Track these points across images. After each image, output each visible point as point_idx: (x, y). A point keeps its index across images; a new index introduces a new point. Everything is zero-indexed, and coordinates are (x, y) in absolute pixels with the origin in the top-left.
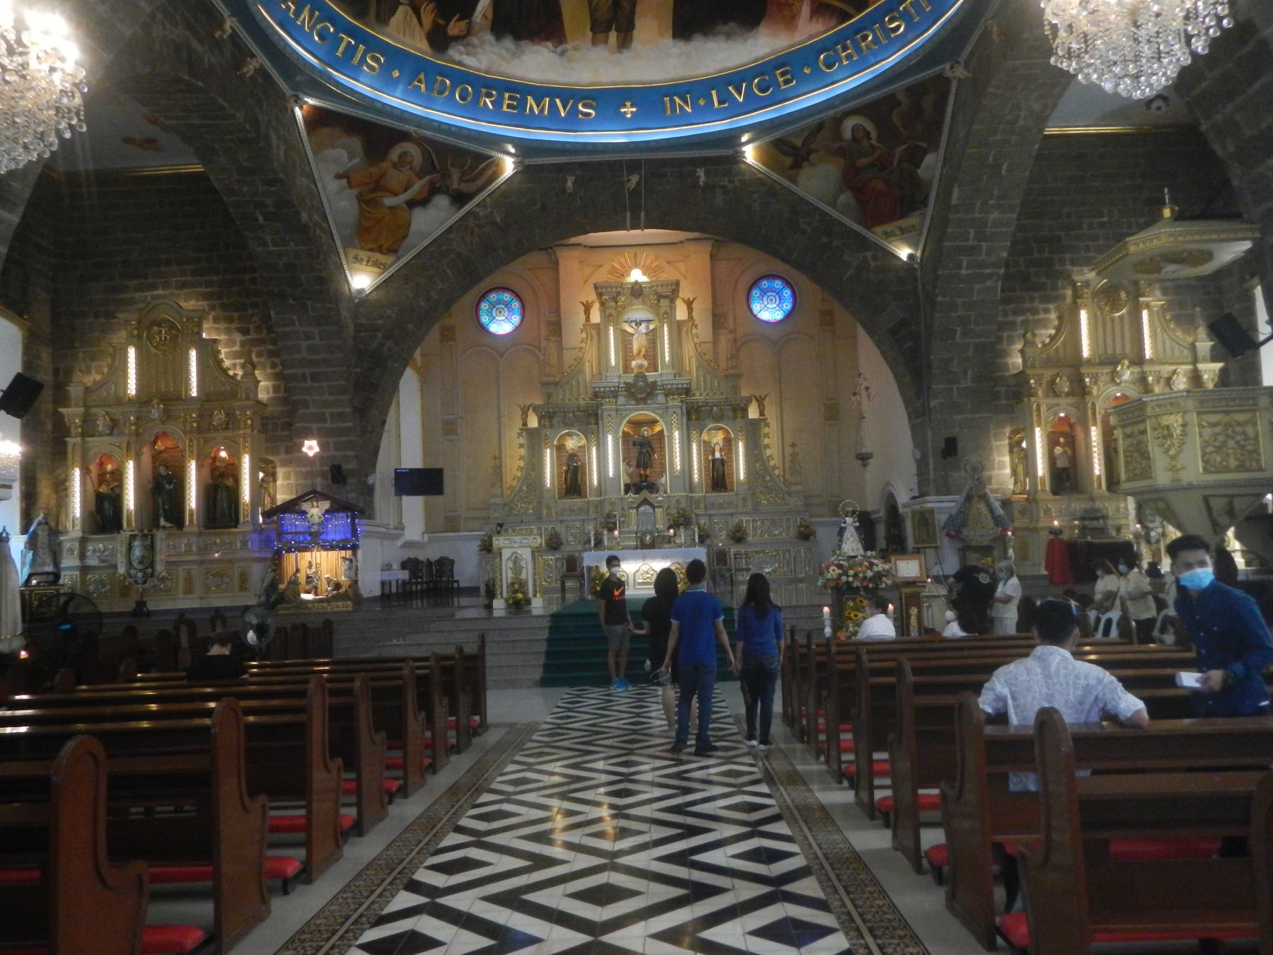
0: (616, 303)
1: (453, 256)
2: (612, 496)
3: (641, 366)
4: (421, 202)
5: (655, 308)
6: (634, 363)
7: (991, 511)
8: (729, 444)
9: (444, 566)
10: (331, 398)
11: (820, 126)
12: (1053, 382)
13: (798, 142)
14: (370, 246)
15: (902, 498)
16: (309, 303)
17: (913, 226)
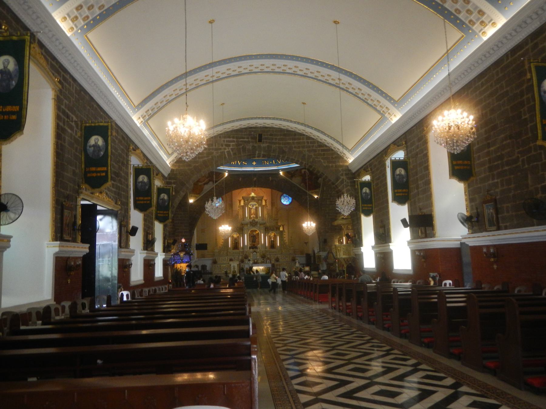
0: (248, 201)
2: (246, 250)
3: (253, 217)
4: (207, 183)
5: (258, 203)
6: (252, 216)
7: (333, 256)
8: (275, 236)
9: (204, 267)
11: (297, 170)
12: (348, 227)
13: (292, 173)
15: (316, 251)
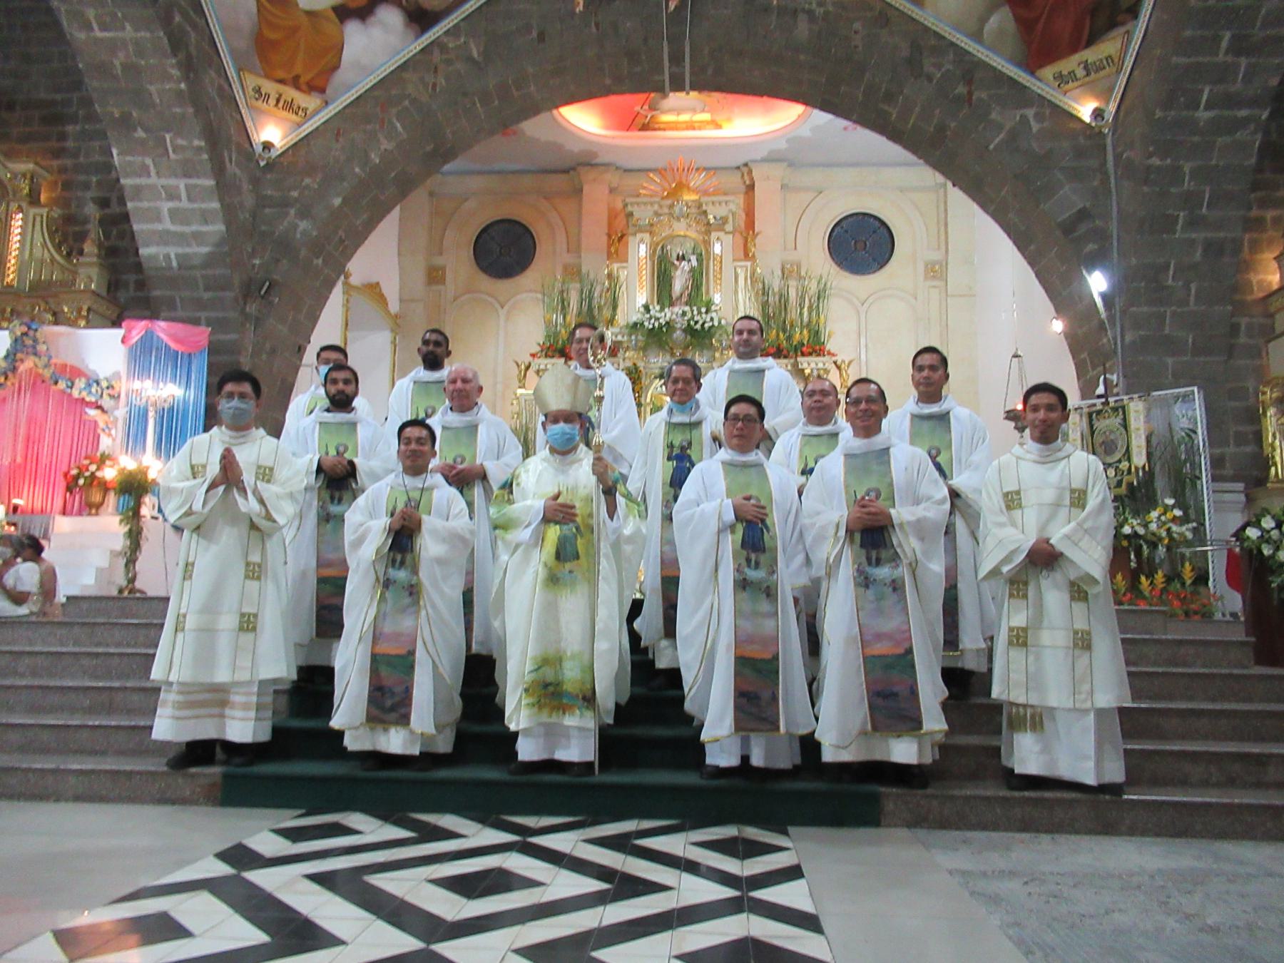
1: (407, 103)
10: (207, 295)
14: (281, 74)
16: (168, 137)
17: (1109, 58)
